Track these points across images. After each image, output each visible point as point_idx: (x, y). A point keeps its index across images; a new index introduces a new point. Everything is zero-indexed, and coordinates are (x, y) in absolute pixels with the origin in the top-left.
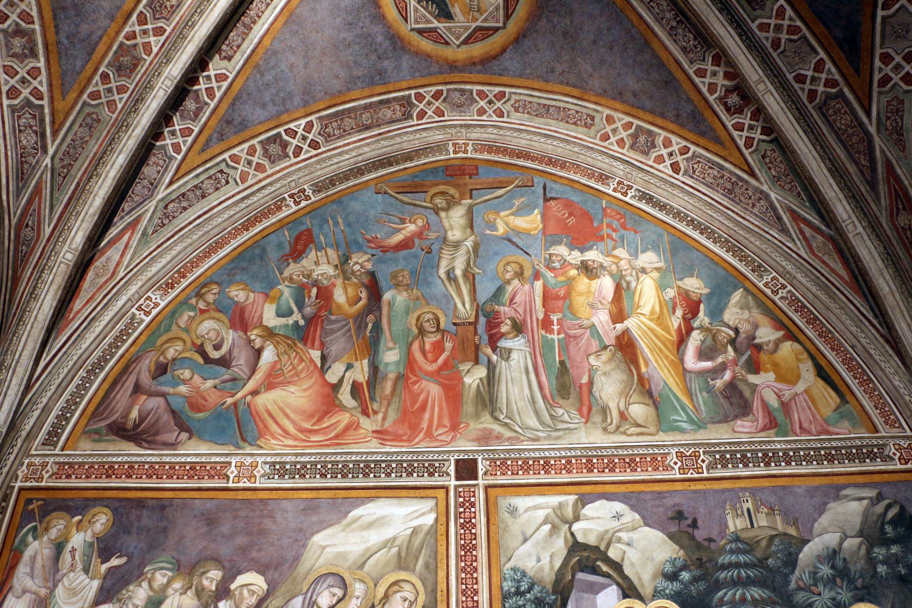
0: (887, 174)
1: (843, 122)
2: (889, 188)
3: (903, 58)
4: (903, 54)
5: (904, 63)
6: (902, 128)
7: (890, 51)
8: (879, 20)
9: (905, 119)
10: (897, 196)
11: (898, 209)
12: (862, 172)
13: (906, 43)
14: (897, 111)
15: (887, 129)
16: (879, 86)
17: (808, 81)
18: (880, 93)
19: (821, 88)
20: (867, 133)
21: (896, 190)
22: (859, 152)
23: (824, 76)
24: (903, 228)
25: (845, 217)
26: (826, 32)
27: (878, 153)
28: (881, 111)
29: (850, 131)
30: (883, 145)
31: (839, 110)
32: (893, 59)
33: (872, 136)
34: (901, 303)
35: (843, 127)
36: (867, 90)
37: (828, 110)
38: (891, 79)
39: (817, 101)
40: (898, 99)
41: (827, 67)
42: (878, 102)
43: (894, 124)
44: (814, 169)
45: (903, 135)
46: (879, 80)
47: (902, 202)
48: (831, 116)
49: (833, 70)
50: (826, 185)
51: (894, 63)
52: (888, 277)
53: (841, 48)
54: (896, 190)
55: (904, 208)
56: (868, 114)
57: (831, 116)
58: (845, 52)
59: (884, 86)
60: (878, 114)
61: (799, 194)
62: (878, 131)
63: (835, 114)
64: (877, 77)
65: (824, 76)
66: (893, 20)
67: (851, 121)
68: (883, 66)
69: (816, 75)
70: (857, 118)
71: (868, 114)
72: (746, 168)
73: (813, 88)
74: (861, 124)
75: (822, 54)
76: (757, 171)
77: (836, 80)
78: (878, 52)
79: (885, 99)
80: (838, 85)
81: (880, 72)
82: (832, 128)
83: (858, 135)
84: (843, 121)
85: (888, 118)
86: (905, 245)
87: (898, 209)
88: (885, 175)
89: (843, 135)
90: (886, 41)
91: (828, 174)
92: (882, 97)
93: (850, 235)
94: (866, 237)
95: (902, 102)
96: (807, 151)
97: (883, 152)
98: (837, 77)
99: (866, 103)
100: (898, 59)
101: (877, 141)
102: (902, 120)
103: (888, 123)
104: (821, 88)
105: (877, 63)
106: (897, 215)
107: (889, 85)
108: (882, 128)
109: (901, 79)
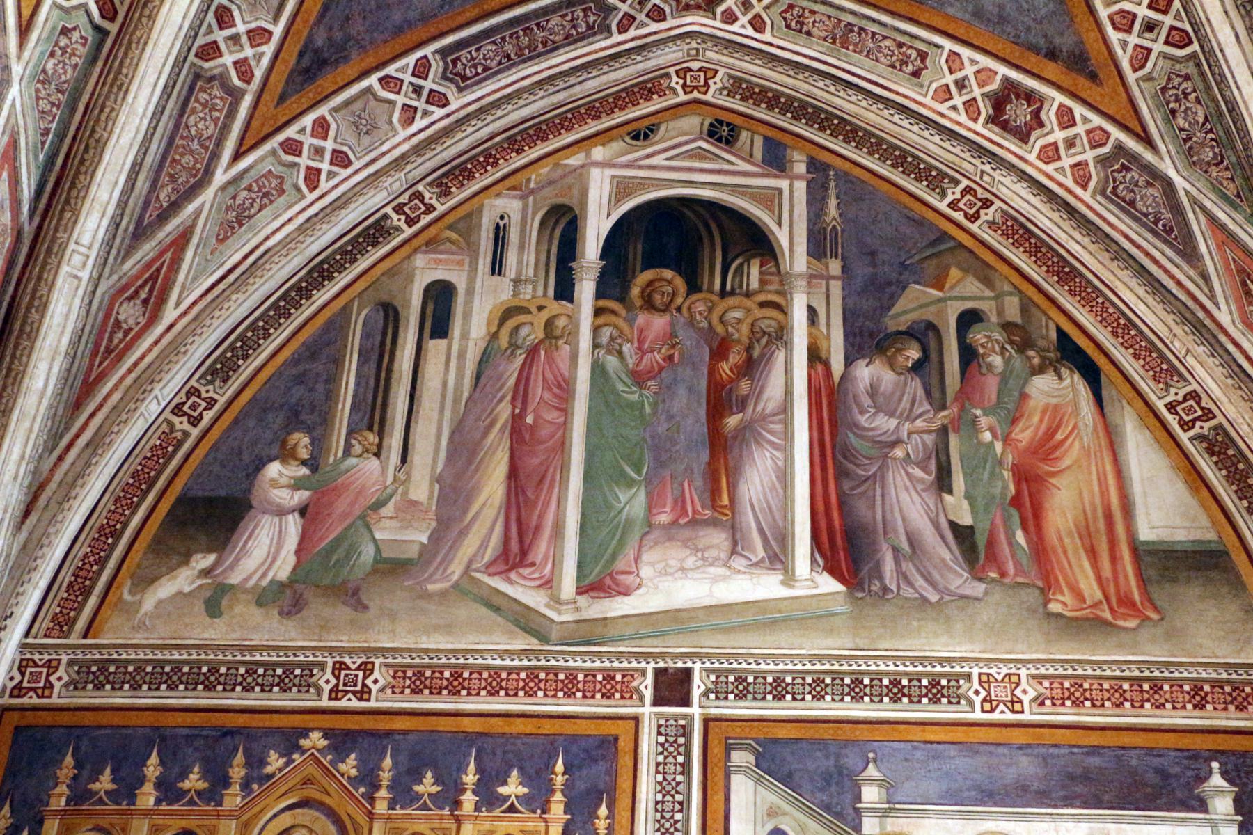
0: (172, 243)
1: (200, 125)
2: (154, 260)
3: (334, 151)
4: (338, 147)
5: (328, 156)
6: (250, 217)
7: (333, 127)
8: (364, 84)
9: (263, 213)
10: (154, 278)
11: (137, 293)
12: (147, 204)
13: (352, 141)
14: (266, 195)
15: (234, 198)
16: (281, 144)
17: (228, 32)
18: (273, 152)
19: (228, 59)
20: (209, 172)
21: (158, 270)
22: (173, 178)
23: (248, 52)
24: (117, 323)
25: (86, 239)
26: (312, 19)
27: (191, 208)
28: (252, 172)
29: (195, 145)
30: (207, 206)
31: (213, 109)
32: (325, 138)
33: (209, 183)
34: (39, 420)
35: (193, 131)
36: (266, 130)
37: (202, 90)
38: (300, 155)
39: (207, 65)
40: (281, 183)
41: (263, 48)
42: (262, 159)
43: (248, 203)
44: (122, 141)
45: (241, 225)
46: (288, 139)
47: (151, 291)
48: (197, 100)
49: (265, 61)
50: (110, 177)
51: (321, 143)
52: (55, 370)
53: (301, 55)
54: (158, 270)
55: (145, 302)
56: (237, 156)
57: (197, 100)
58: (298, 62)
59: (286, 153)
60: (246, 171)
61: (46, 132)
62: (223, 188)
63: (205, 105)
64: (291, 132)
65: (248, 52)
66: (372, 103)
67: (209, 138)
68: (309, 130)
69: (244, 39)
70: (219, 143)
71: (237, 156)
72: (26, 13)
73: (223, 46)
74: (215, 156)
75: (278, 30)
76: (34, 36)
77: (253, 75)
78: (323, 110)
79: (268, 165)
80: (248, 82)
81: (299, 132)
82: (181, 115)
83: (196, 161)
84: (200, 124)
85: (249, 189)
86: (97, 345)
87: (137, 293)
88: (168, 240)
89: (182, 138)
90: (343, 111)
91: (127, 167)
92: (271, 159)
93: (65, 269)
94: (80, 292)
95: (282, 192)
96: (141, 111)
97: (198, 213)
98: (259, 74)
99: (249, 142)
100: (329, 145)
101: (207, 196)
102: (260, 210)
103: (244, 194)
104: (228, 59)
105: (308, 120)
106: (130, 299)
107: (291, 158)
108: (231, 190)
109: (308, 168)
